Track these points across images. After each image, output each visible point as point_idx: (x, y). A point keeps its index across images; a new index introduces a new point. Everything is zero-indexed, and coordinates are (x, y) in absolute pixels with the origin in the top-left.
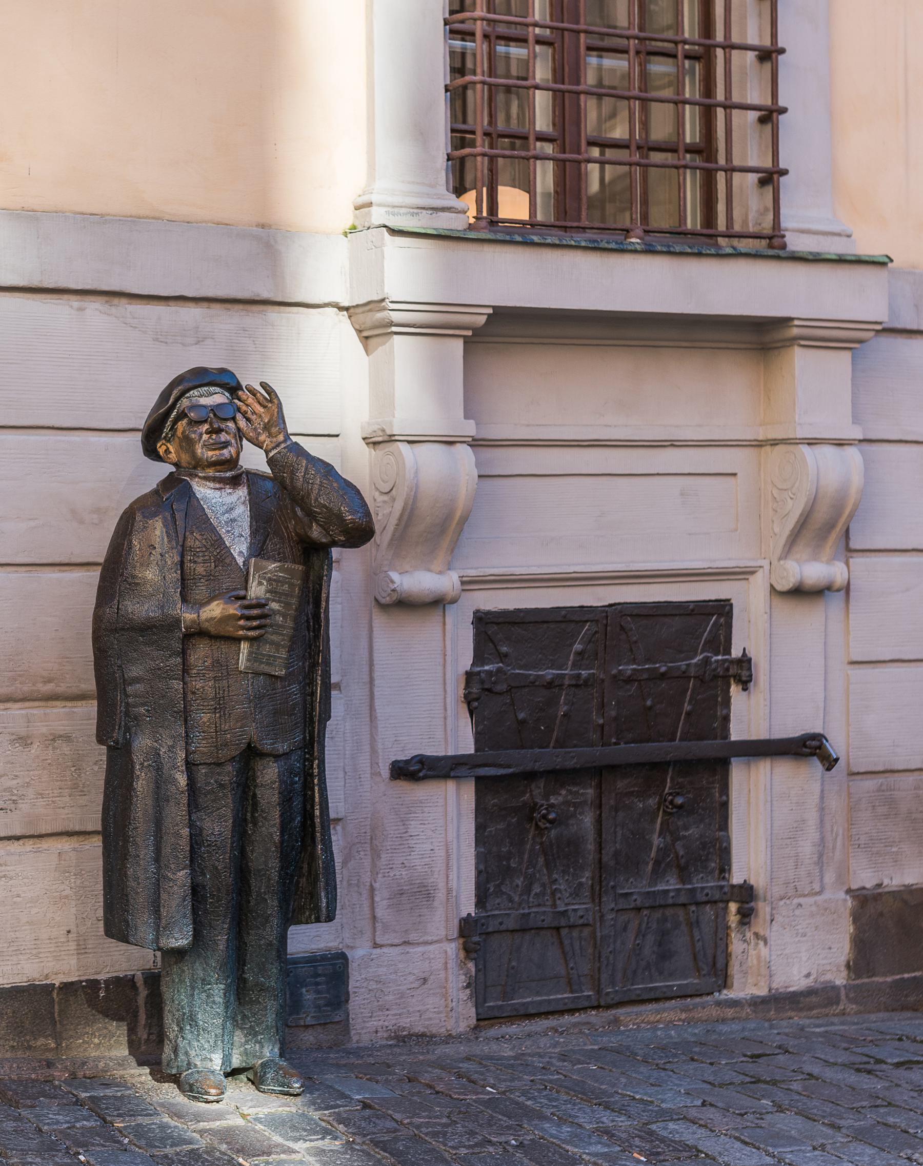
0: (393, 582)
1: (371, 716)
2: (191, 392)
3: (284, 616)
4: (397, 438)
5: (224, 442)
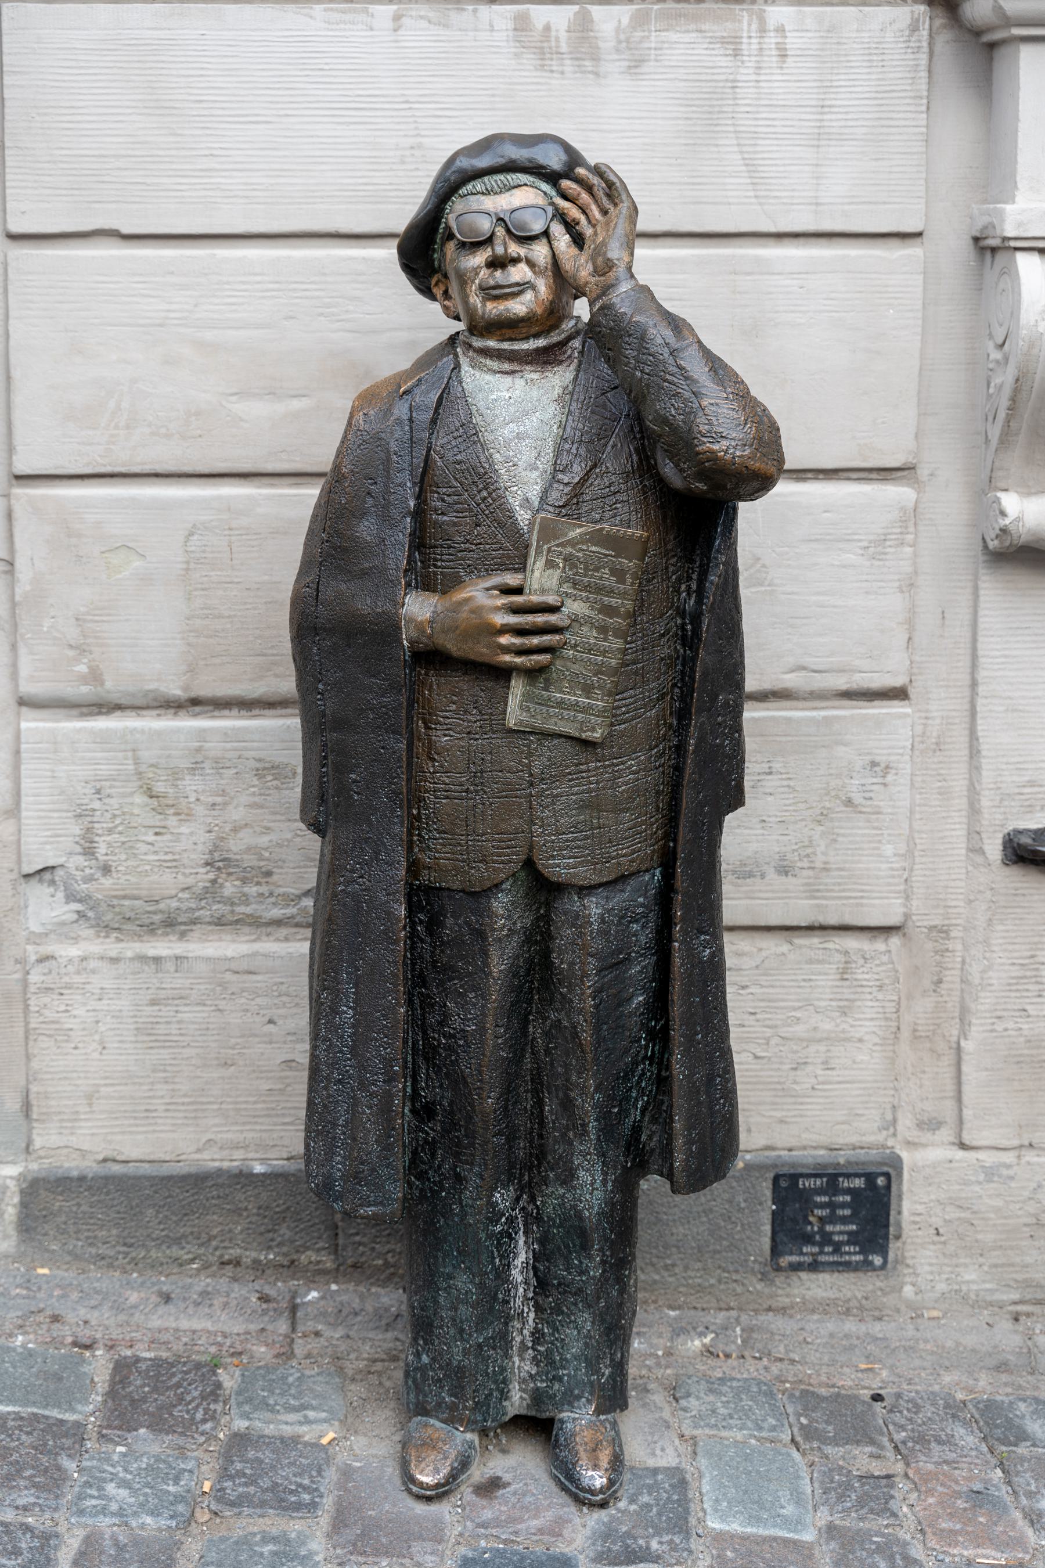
0: (1003, 514)
1: (971, 747)
2: (470, 187)
3: (603, 630)
4: (1013, 244)
5: (518, 284)
